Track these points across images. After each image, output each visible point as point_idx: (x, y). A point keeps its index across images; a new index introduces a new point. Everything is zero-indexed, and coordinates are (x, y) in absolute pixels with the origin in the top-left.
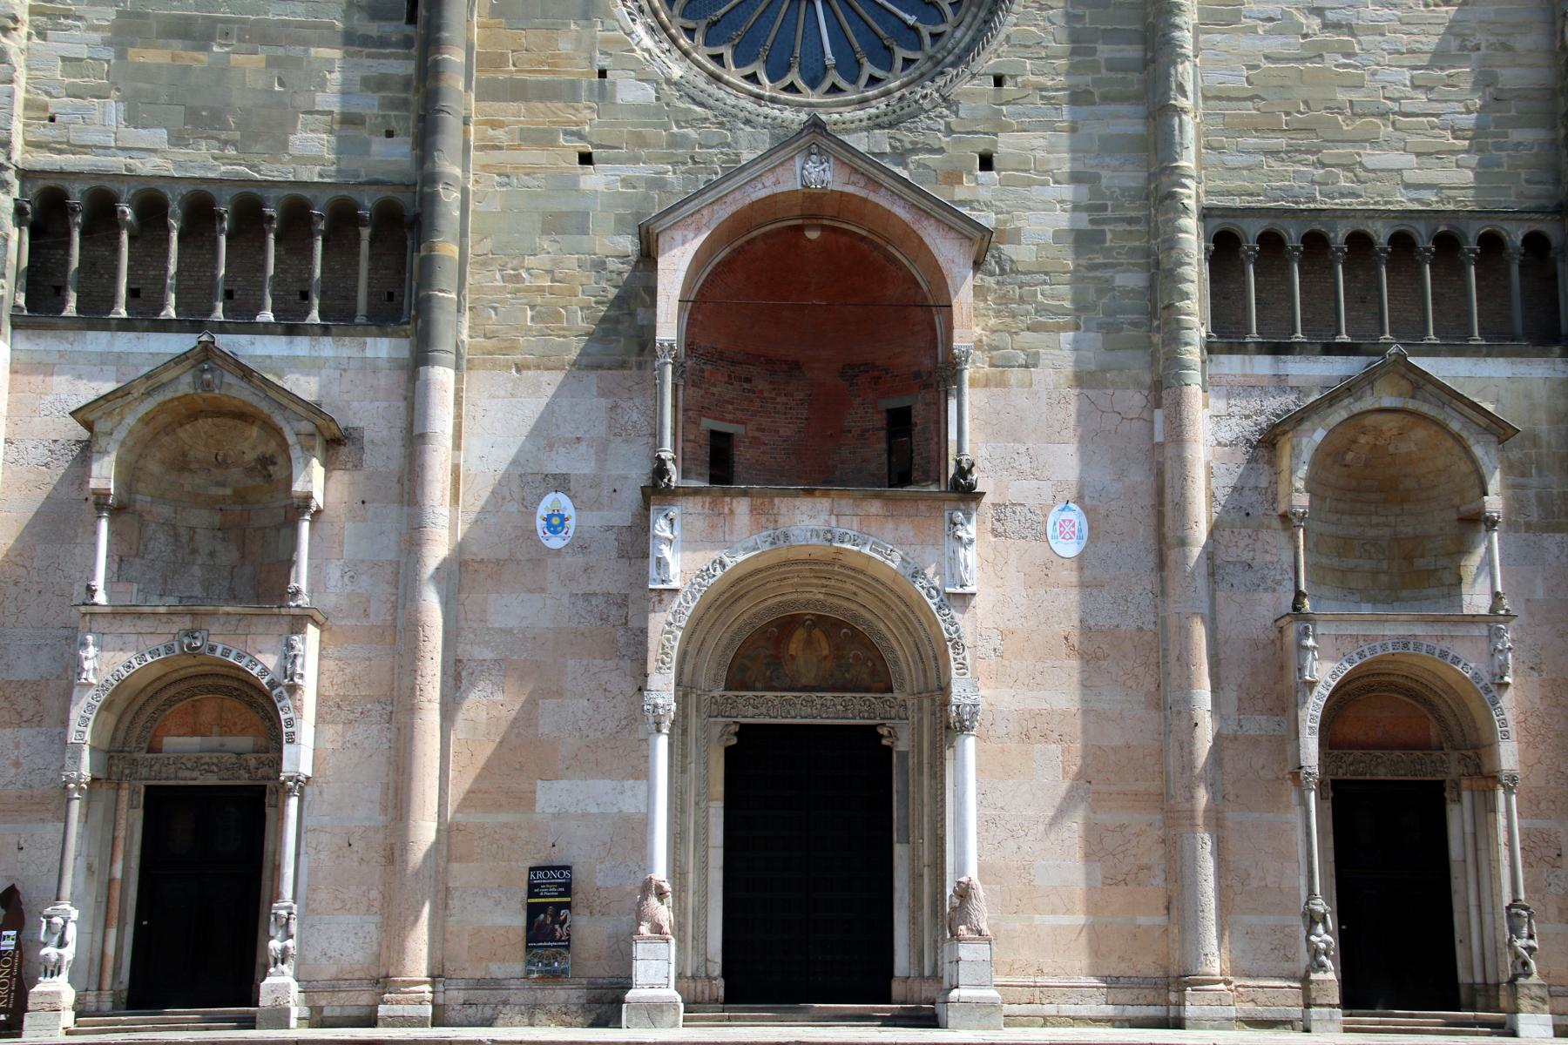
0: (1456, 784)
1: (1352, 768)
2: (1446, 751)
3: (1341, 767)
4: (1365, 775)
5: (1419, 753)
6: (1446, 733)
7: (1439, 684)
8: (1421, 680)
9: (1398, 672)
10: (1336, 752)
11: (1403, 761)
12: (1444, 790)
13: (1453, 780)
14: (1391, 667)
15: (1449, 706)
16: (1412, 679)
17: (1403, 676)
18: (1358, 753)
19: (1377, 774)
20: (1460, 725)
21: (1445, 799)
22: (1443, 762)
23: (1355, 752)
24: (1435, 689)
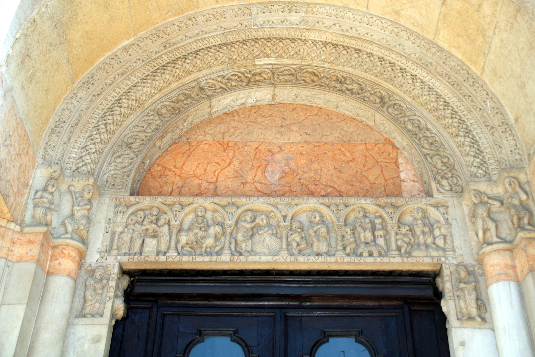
0: (469, 273)
1: (183, 239)
2: (438, 197)
3: (155, 237)
4: (218, 253)
5: (368, 204)
6: (437, 161)
7: (409, 47)
8: (369, 48)
9: (313, 36)
10: (146, 201)
11: (323, 221)
12: (439, 295)
13: (458, 265)
14: (295, 18)
15: (438, 96)
16: (346, 48)
17: (325, 44)
18: (208, 203)
19: (252, 252)
20: (468, 132)
21: (443, 318)
22: (430, 226)
23: (199, 201)
24: (402, 62)
